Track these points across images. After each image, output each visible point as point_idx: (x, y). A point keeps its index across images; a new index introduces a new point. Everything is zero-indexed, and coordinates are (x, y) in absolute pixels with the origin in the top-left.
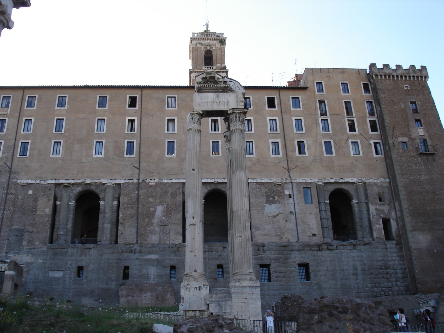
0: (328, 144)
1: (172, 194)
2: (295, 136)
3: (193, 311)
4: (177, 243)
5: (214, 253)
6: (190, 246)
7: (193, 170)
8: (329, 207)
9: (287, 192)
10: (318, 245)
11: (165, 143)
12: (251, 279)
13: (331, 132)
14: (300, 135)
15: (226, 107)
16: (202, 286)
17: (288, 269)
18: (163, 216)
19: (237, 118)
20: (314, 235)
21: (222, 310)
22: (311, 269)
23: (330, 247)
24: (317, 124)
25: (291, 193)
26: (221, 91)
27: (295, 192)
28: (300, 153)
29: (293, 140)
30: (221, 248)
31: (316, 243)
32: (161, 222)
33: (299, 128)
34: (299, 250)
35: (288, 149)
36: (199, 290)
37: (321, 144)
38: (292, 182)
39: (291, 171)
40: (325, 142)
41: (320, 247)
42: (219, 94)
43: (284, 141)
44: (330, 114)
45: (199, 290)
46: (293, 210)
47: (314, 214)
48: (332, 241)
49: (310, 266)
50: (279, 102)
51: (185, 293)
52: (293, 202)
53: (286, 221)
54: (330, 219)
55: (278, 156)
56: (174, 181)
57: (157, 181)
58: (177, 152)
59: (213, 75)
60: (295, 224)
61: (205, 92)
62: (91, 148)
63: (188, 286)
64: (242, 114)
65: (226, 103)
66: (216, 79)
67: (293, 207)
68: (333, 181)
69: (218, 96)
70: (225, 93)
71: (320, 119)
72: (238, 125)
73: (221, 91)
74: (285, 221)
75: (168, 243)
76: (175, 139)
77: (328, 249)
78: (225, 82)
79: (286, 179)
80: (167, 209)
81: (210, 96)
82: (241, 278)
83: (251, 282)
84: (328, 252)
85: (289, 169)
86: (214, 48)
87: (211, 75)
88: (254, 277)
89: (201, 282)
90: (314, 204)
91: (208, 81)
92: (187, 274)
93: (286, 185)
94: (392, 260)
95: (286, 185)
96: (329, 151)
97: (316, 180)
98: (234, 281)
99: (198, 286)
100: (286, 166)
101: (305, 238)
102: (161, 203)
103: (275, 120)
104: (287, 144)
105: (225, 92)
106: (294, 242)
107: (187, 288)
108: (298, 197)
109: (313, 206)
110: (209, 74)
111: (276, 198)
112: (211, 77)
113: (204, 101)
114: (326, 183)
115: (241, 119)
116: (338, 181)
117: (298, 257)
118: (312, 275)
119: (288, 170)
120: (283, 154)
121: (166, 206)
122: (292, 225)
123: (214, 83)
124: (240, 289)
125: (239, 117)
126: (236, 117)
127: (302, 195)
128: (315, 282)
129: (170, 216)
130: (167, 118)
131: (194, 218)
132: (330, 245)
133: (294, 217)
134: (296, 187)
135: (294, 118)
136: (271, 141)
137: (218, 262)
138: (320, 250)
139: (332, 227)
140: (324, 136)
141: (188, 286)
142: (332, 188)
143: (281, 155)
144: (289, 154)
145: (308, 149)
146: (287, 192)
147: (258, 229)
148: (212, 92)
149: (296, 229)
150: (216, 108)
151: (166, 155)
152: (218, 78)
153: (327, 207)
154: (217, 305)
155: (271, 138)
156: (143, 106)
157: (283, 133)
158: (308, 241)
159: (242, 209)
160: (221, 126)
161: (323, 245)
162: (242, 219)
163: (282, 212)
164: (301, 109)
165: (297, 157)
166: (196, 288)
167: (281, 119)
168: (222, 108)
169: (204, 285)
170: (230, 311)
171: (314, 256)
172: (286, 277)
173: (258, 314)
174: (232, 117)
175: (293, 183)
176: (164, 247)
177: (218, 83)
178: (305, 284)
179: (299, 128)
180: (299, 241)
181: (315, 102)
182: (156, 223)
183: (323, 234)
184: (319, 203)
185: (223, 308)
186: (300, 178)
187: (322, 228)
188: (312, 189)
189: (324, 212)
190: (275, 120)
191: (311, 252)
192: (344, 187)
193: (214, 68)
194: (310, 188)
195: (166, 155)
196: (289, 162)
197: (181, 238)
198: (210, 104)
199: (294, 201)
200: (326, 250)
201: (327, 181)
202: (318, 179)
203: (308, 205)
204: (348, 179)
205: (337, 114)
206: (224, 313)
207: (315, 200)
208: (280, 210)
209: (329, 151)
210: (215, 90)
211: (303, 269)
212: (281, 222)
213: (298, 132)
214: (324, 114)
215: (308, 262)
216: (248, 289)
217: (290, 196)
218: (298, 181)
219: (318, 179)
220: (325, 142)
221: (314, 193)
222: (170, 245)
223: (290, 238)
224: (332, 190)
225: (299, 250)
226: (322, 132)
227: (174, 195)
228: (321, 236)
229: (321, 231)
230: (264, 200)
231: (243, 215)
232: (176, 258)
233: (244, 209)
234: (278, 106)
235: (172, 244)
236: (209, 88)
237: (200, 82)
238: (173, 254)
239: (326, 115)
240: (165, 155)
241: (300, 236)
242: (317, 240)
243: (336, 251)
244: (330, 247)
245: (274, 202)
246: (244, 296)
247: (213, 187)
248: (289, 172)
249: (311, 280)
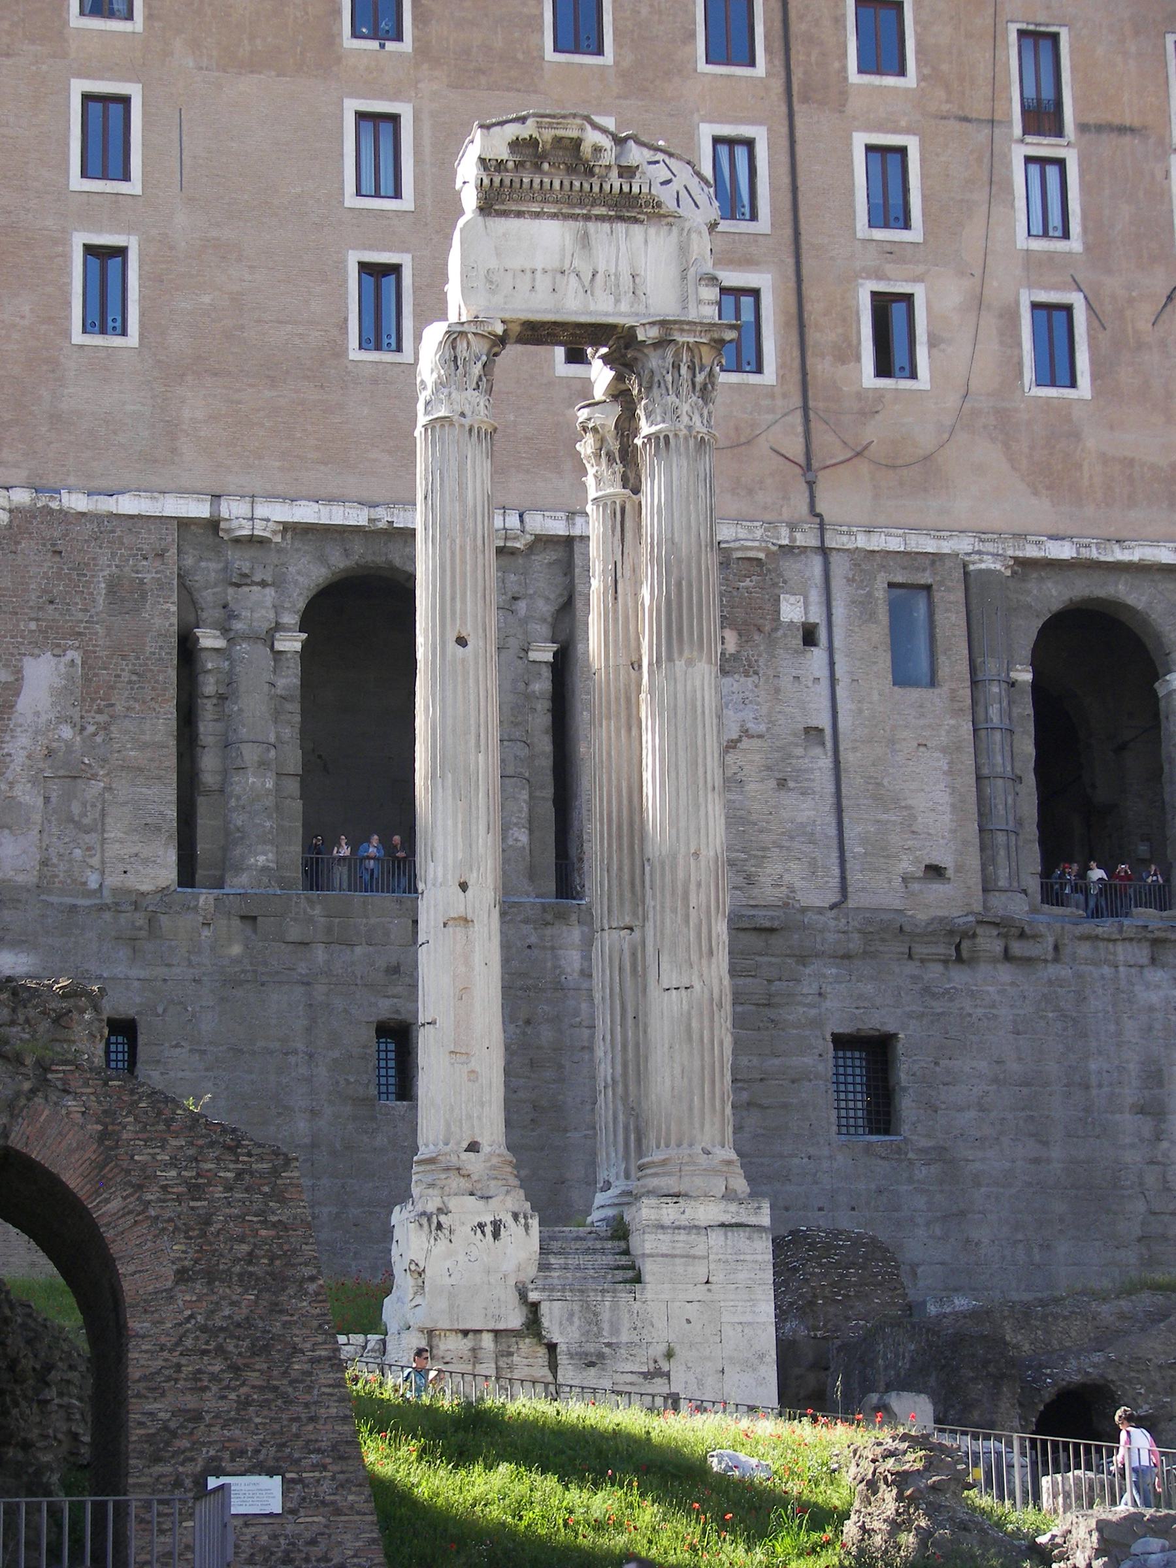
0: (1053, 320)
1: (113, 588)
2: (859, 259)
3: (465, 1333)
4: (145, 888)
5: (358, 950)
6: (445, 1022)
7: (462, 641)
8: (1030, 711)
9: (792, 611)
10: (951, 933)
11: (67, 257)
12: (729, 1196)
13: (1075, 244)
14: (891, 251)
15: (624, 307)
16: (508, 1219)
17: (777, 1061)
18: (62, 719)
19: (684, 370)
20: (935, 871)
21: (599, 1334)
22: (905, 1071)
23: (1017, 948)
24: (997, 184)
25: (816, 616)
26: (602, 211)
27: (839, 611)
28: (884, 368)
29: (850, 279)
31: (942, 919)
32: (50, 754)
33: (890, 209)
34: (847, 956)
35: (812, 336)
36: (496, 1235)
37: (1011, 317)
38: (824, 551)
39: (824, 482)
40: (1035, 306)
41: (965, 945)
42: (591, 226)
43: (792, 284)
44: (1083, 128)
45: (496, 1235)
46: (823, 721)
47: (944, 750)
48: (1034, 910)
49: (900, 1048)
50: (778, 25)
51: (429, 1251)
52: (824, 673)
53: (782, 783)
54: (1030, 779)
55: (753, 379)
56: (127, 505)
57: (22, 497)
58: (142, 314)
59: (573, 134)
60: (830, 800)
61: (519, 214)
63: (442, 1218)
64: (705, 350)
65: (626, 280)
66: (586, 149)
67: (826, 703)
68: (1064, 551)
69: (585, 241)
70: (620, 227)
71: (1018, 153)
72: (685, 408)
73: (602, 211)
74: (772, 783)
75: (93, 885)
76: (129, 229)
77: (1007, 956)
79: (793, 527)
80: (87, 679)
81: (544, 238)
82: (683, 1189)
83: (733, 1207)
84: (1005, 973)
85: (815, 464)
87: (561, 133)
88: (741, 1185)
89: (508, 1202)
90: (944, 690)
91: (543, 157)
92: (431, 1161)
93: (790, 568)
95: (790, 568)
96: (1057, 366)
97: (963, 545)
98: (653, 1201)
99: (488, 1219)
100: (795, 447)
101: (880, 889)
102: (49, 639)
103: (749, 143)
104: (808, 307)
105: (621, 219)
106: (820, 911)
107: (439, 1226)
108: (860, 643)
109: (935, 699)
110: (550, 126)
112: (558, 140)
113: (516, 263)
114: (1025, 565)
115: (700, 378)
116: (1094, 554)
117: (840, 1001)
118: (907, 1106)
119: (809, 469)
120: (781, 366)
121: (77, 656)
122: (813, 810)
123: (571, 170)
124: (682, 1236)
125: (692, 368)
126: (676, 366)
127: (879, 631)
128: (924, 1143)
129: (101, 718)
130: (79, 87)
131: (464, 887)
132: (1022, 935)
133: (826, 762)
134: (851, 581)
135: (860, 140)
137: (384, 1009)
138: (959, 959)
139: (1041, 825)
140: (1034, 266)
141: (442, 1218)
142: (1055, 595)
143: (769, 376)
144: (821, 367)
145: (932, 344)
146: (792, 611)
148: (554, 216)
149: (833, 832)
150: (576, 306)
151: (78, 337)
152: (597, 149)
153: (1016, 711)
154: (576, 1307)
157: (788, 232)
158: (897, 904)
159: (696, 854)
160: (417, 162)
161: (980, 931)
162: (693, 902)
163: (762, 728)
164: (910, 80)
165: (861, 395)
166: (481, 1226)
167: (784, 143)
168: (602, 308)
169: (516, 1216)
170: (636, 1339)
171: (926, 990)
172: (761, 1107)
173: (761, 1357)
174: (654, 361)
175: (834, 558)
176: (73, 908)
177: (590, 172)
178: (868, 1149)
179: (890, 209)
180: (851, 904)
181: (996, 37)
182: (20, 758)
183: (983, 870)
184: (974, 683)
185: (606, 1326)
186: (872, 524)
187: (981, 830)
188: (937, 596)
189: (997, 736)
190: (749, 143)
191: (911, 968)
192: (1122, 590)
194: (928, 588)
195: (78, 337)
196: (816, 426)
197: (172, 856)
198: (544, 284)
199: (832, 664)
200: (994, 961)
201: (1031, 552)
202: (981, 534)
203: (914, 694)
204: (1155, 542)
205: (1122, 130)
206: (608, 1345)
207: (954, 664)
209: (1057, 366)
210: (573, 206)
211: (857, 1060)
212: (751, 787)
213: (880, 234)
214: (1043, 117)
215: (891, 1028)
216: (716, 1239)
217: (809, 637)
218: (862, 542)
219: (981, 534)
220: (1035, 306)
221: (951, 620)
222: (108, 899)
223: (799, 884)
224: (1056, 606)
225: (847, 956)
226: (1022, 241)
227: (126, 595)
228: (975, 880)
229: (974, 850)
231: (699, 885)
232: (135, 972)
233: (703, 852)
234: (768, 49)
235: (115, 891)
237: (500, 165)
238: (123, 953)
239: (1060, 133)
240: (67, 334)
241: (855, 877)
242: (948, 901)
243: (1052, 970)
244: (1017, 948)
246: (701, 1271)
247: (360, 554)
248: (811, 484)
249: (905, 1129)
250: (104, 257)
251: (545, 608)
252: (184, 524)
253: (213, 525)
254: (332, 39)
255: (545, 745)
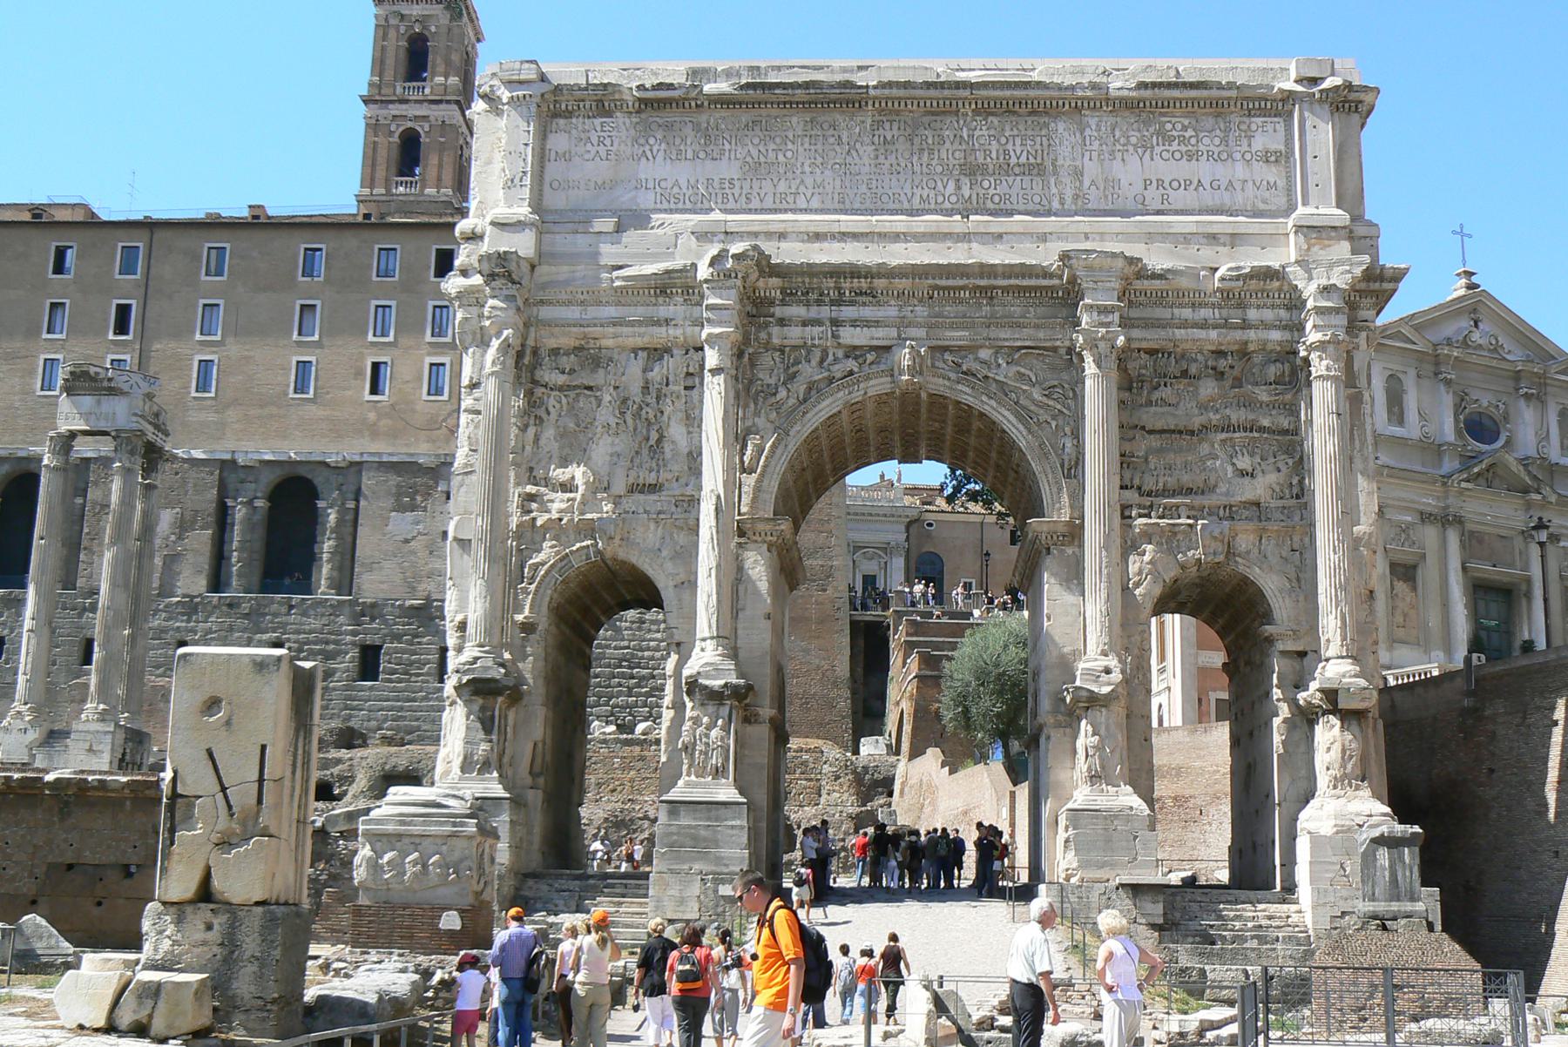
30: (284, 610)
62: (32, 372)
69: (99, 402)
78: (110, 380)
86: (433, 29)
94: (648, 649)
111: (419, 498)
136: (428, 360)
147: (370, 568)
155: (429, 354)
156: (153, 271)
193: (427, 91)
208: (420, 527)
230: (389, 502)
236: (84, 389)
245: (413, 508)
250: (205, 365)
251: (353, 488)
252: (223, 462)
253: (234, 462)
254: (294, 277)
255: (349, 539)
